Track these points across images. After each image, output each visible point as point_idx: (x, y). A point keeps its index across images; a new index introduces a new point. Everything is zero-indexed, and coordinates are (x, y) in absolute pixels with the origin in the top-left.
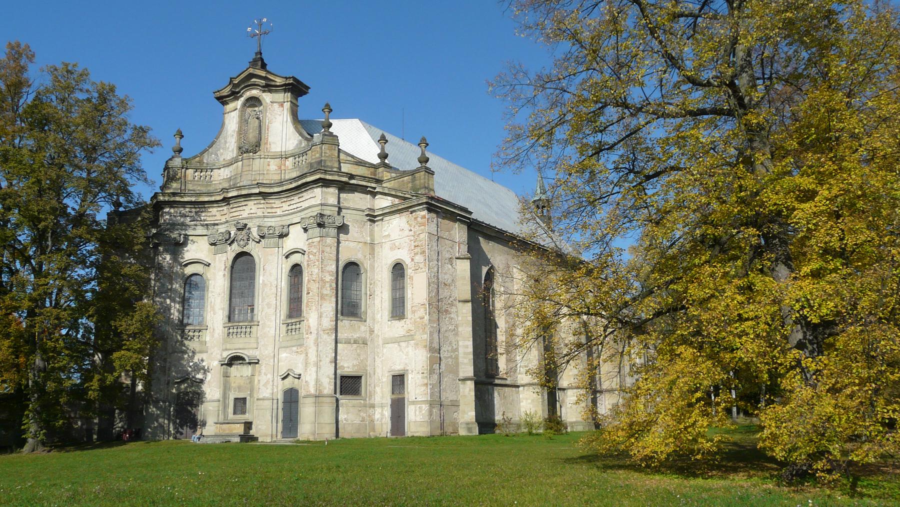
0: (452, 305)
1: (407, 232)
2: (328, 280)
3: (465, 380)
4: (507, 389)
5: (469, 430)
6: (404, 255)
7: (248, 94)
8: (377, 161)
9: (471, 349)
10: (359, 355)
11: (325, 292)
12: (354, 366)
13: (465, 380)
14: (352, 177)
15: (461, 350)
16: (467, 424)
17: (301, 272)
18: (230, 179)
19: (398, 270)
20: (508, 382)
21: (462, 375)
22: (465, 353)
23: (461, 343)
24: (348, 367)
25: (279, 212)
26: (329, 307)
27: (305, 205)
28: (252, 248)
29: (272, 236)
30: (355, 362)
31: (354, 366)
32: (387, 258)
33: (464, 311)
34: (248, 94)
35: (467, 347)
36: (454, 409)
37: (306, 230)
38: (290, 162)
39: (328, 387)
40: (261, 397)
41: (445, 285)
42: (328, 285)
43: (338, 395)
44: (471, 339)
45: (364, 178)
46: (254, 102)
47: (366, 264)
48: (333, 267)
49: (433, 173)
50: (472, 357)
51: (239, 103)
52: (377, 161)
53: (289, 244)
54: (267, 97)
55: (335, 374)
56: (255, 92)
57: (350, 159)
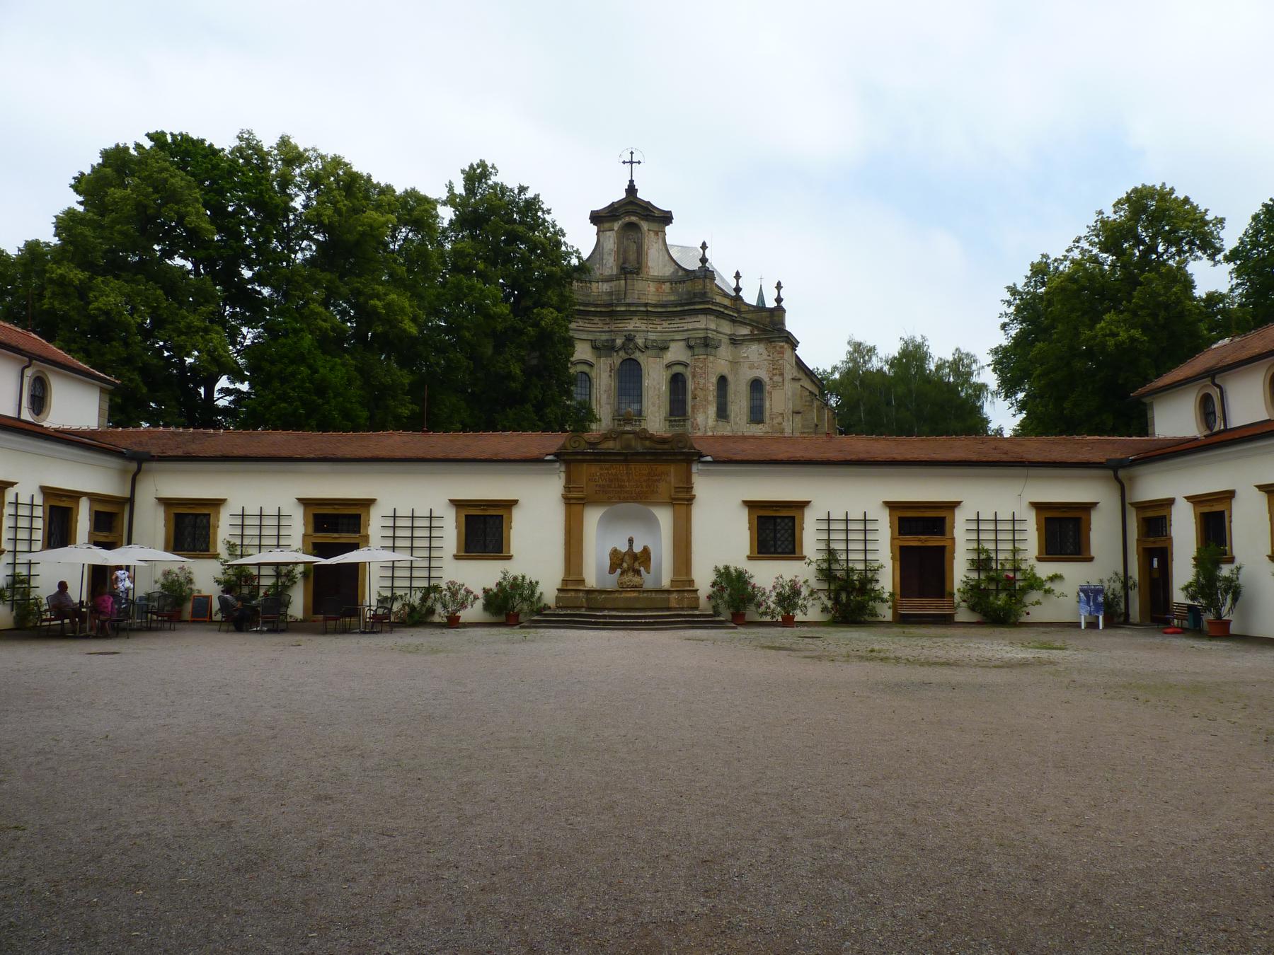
1: (765, 357)
6: (763, 374)
7: (627, 219)
8: (733, 294)
17: (684, 382)
18: (610, 294)
19: (756, 385)
25: (659, 328)
27: (686, 326)
28: (637, 355)
29: (654, 348)
32: (748, 374)
34: (627, 219)
37: (690, 347)
38: (667, 287)
45: (726, 307)
46: (632, 227)
47: (730, 378)
51: (616, 226)
52: (733, 294)
53: (670, 356)
54: (645, 226)
56: (633, 219)
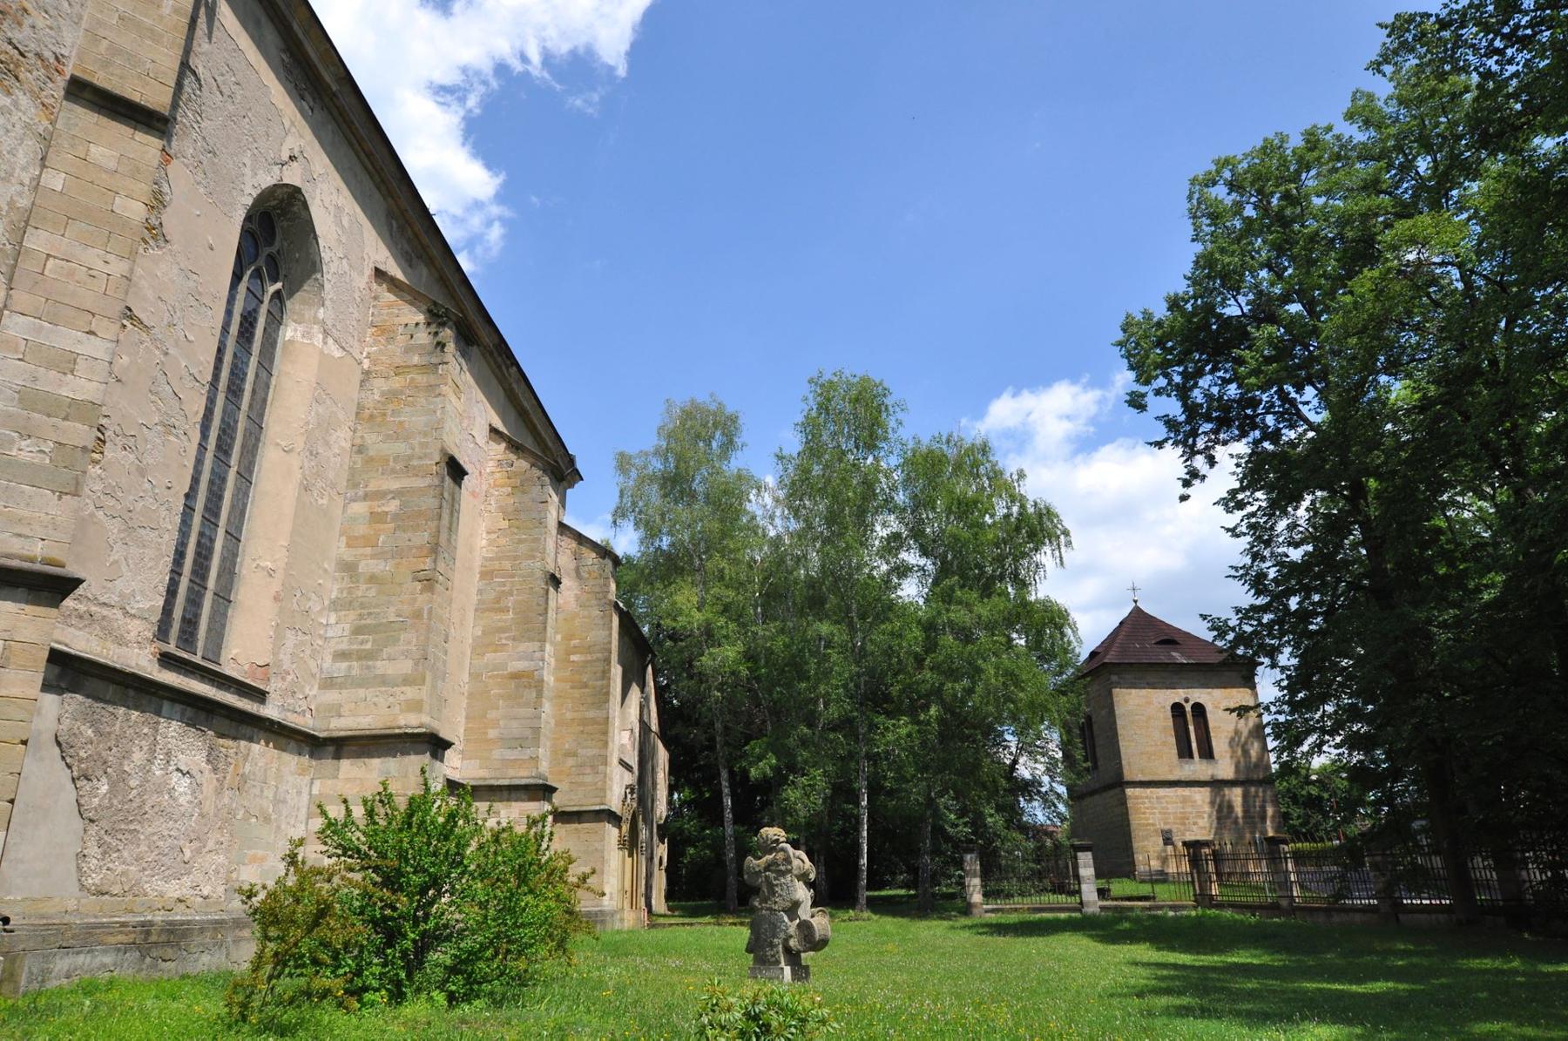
20: (270, 711)
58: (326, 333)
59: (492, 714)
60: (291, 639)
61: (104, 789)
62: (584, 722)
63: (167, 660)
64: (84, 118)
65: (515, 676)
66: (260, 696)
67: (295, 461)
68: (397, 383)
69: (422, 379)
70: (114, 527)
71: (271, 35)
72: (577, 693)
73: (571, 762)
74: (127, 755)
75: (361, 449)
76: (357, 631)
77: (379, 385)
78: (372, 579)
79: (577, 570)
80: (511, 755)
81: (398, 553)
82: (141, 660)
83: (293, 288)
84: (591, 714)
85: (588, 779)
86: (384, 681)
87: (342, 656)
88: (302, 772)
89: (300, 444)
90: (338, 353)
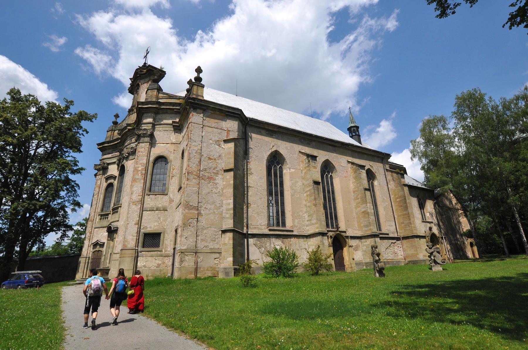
0: (217, 174)
2: (140, 169)
3: (224, 232)
4: (293, 240)
5: (227, 274)
9: (232, 206)
10: (159, 218)
11: (137, 177)
12: (154, 226)
13: (224, 232)
14: (163, 104)
15: (224, 207)
16: (225, 269)
20: (294, 233)
21: (224, 228)
22: (227, 210)
23: (224, 202)
24: (150, 226)
26: (138, 188)
30: (156, 224)
31: (154, 226)
33: (228, 177)
35: (229, 204)
36: (217, 255)
39: (132, 243)
40: (116, 252)
41: (210, 159)
42: (139, 172)
43: (140, 249)
44: (232, 198)
48: (145, 161)
49: (203, 86)
50: (232, 212)
55: (139, 232)
57: (165, 95)
58: (290, 169)
59: (361, 221)
60: (296, 221)
61: (263, 249)
62: (403, 215)
63: (270, 230)
64: (226, 173)
65: (363, 212)
66: (292, 231)
67: (289, 192)
68: (305, 170)
69: (308, 168)
70: (256, 215)
71: (263, 132)
72: (400, 208)
73: (403, 225)
74: (266, 244)
75: (303, 184)
76: (309, 216)
77: (304, 172)
78: (309, 207)
79: (393, 179)
80: (366, 229)
81: (311, 201)
82: (266, 232)
83: (282, 164)
84: (405, 213)
85: (408, 228)
86: (313, 224)
87: (308, 221)
88: (305, 241)
89: (289, 189)
90: (293, 170)
